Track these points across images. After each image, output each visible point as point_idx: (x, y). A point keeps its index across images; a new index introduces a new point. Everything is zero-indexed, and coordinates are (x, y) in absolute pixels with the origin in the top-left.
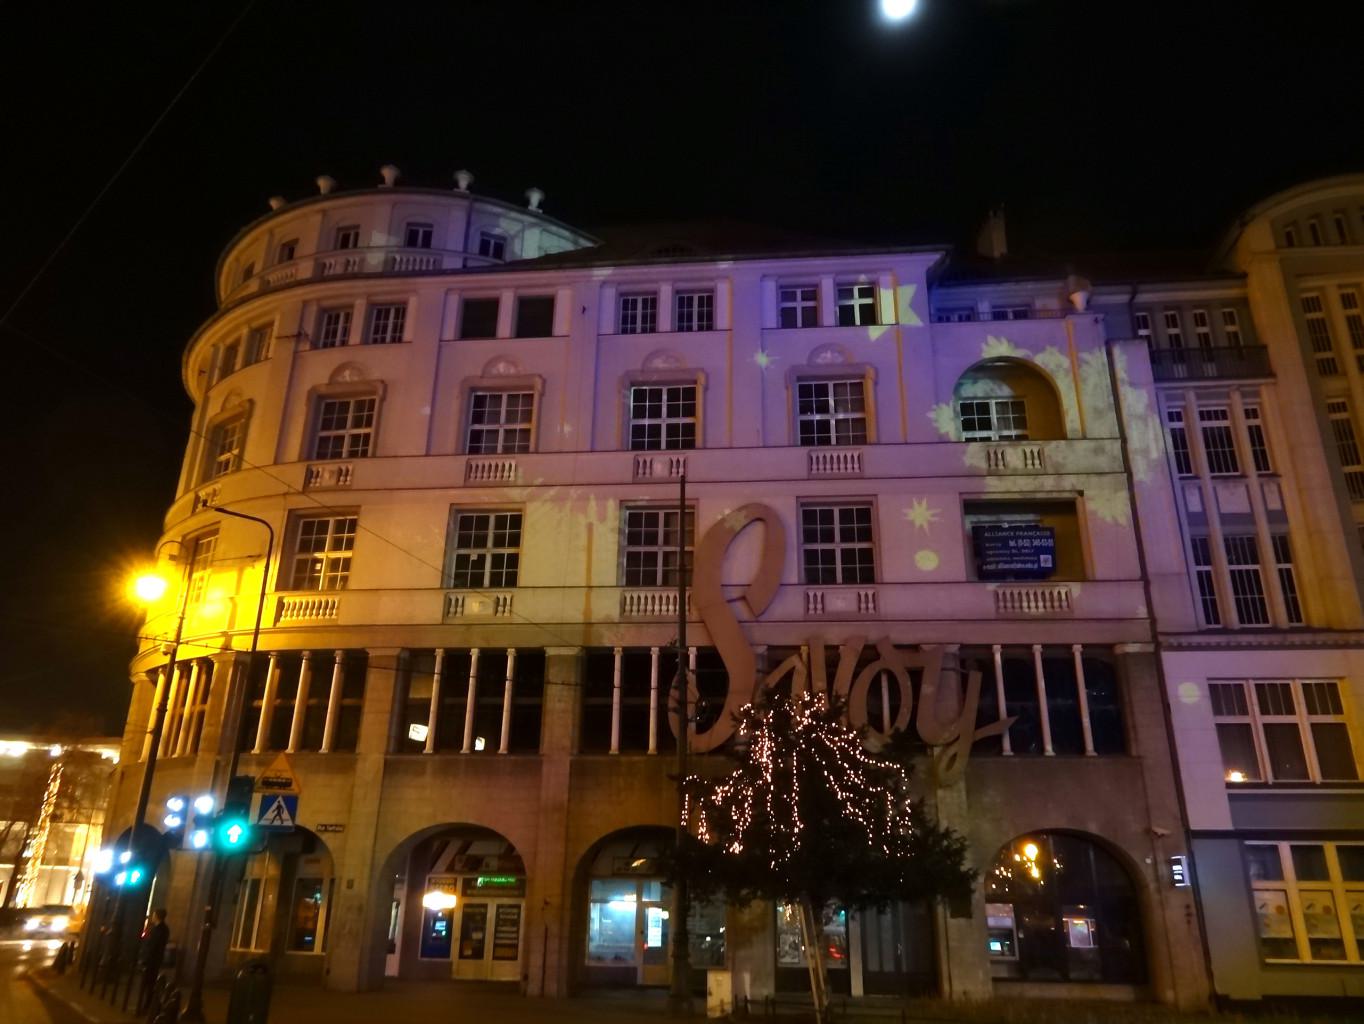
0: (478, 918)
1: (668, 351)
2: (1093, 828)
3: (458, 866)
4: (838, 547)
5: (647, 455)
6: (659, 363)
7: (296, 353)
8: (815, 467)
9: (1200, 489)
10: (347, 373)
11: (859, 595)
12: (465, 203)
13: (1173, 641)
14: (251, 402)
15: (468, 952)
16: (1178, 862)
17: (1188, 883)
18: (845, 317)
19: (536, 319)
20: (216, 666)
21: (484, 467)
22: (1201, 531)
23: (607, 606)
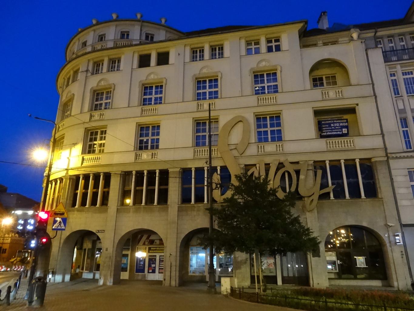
0: (154, 260)
1: (208, 66)
2: (365, 224)
3: (146, 243)
4: (269, 129)
5: (201, 102)
6: (205, 71)
7: (86, 77)
8: (260, 102)
9: (403, 100)
10: (102, 82)
11: (277, 145)
12: (140, 23)
13: (394, 155)
14: (74, 94)
15: (151, 271)
16: (398, 235)
17: (402, 243)
18: (270, 50)
19: (163, 59)
20: (64, 180)
21: (147, 110)
22: (403, 116)
23: (189, 154)
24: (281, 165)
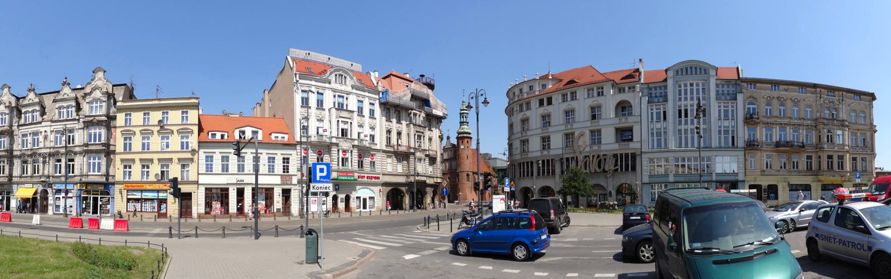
18: (599, 95)
24: (599, 156)
